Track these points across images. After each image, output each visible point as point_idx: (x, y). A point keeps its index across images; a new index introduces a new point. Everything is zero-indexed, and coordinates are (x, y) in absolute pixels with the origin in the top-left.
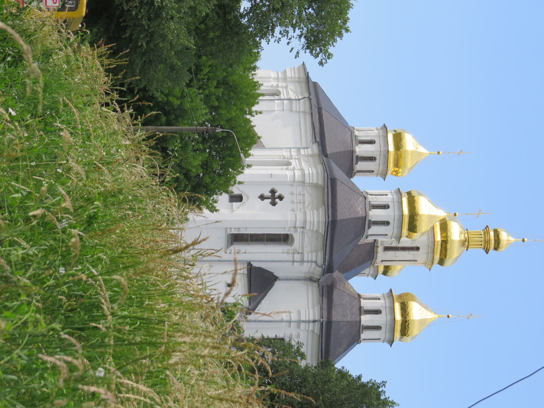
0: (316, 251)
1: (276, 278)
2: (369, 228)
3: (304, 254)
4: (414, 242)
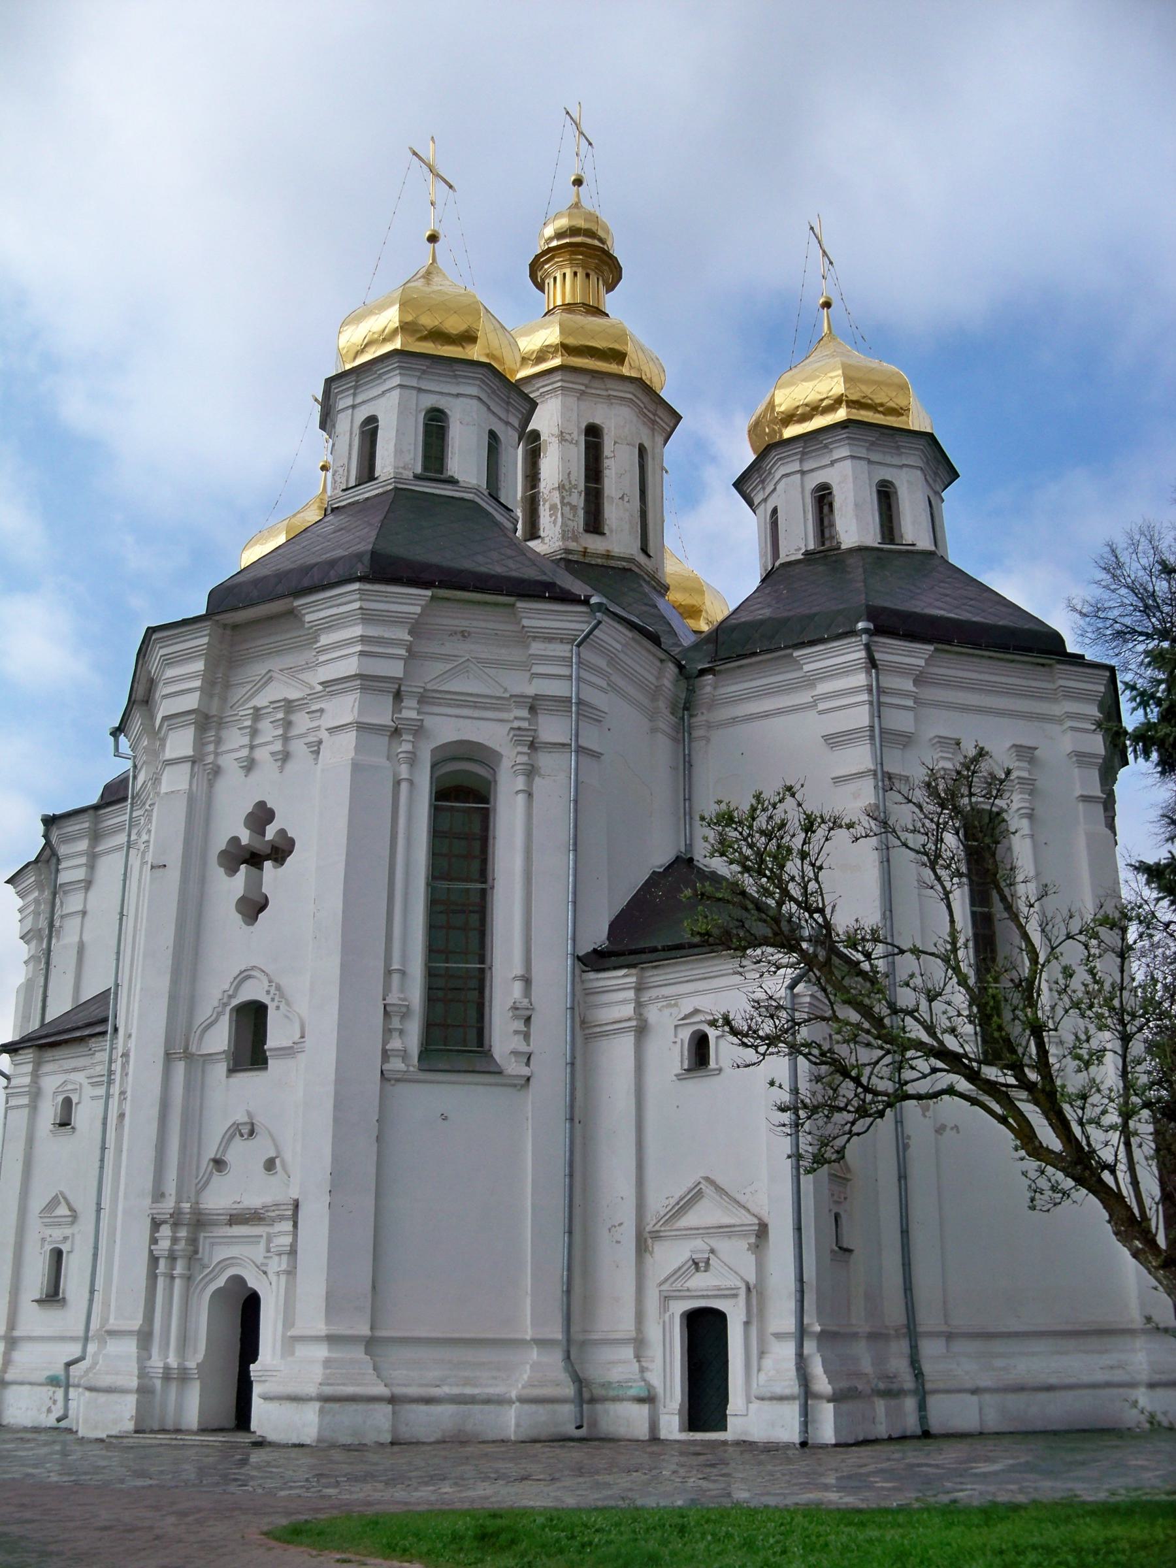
0: (525, 637)
1: (684, 863)
2: (452, 481)
3: (536, 697)
4: (568, 437)
